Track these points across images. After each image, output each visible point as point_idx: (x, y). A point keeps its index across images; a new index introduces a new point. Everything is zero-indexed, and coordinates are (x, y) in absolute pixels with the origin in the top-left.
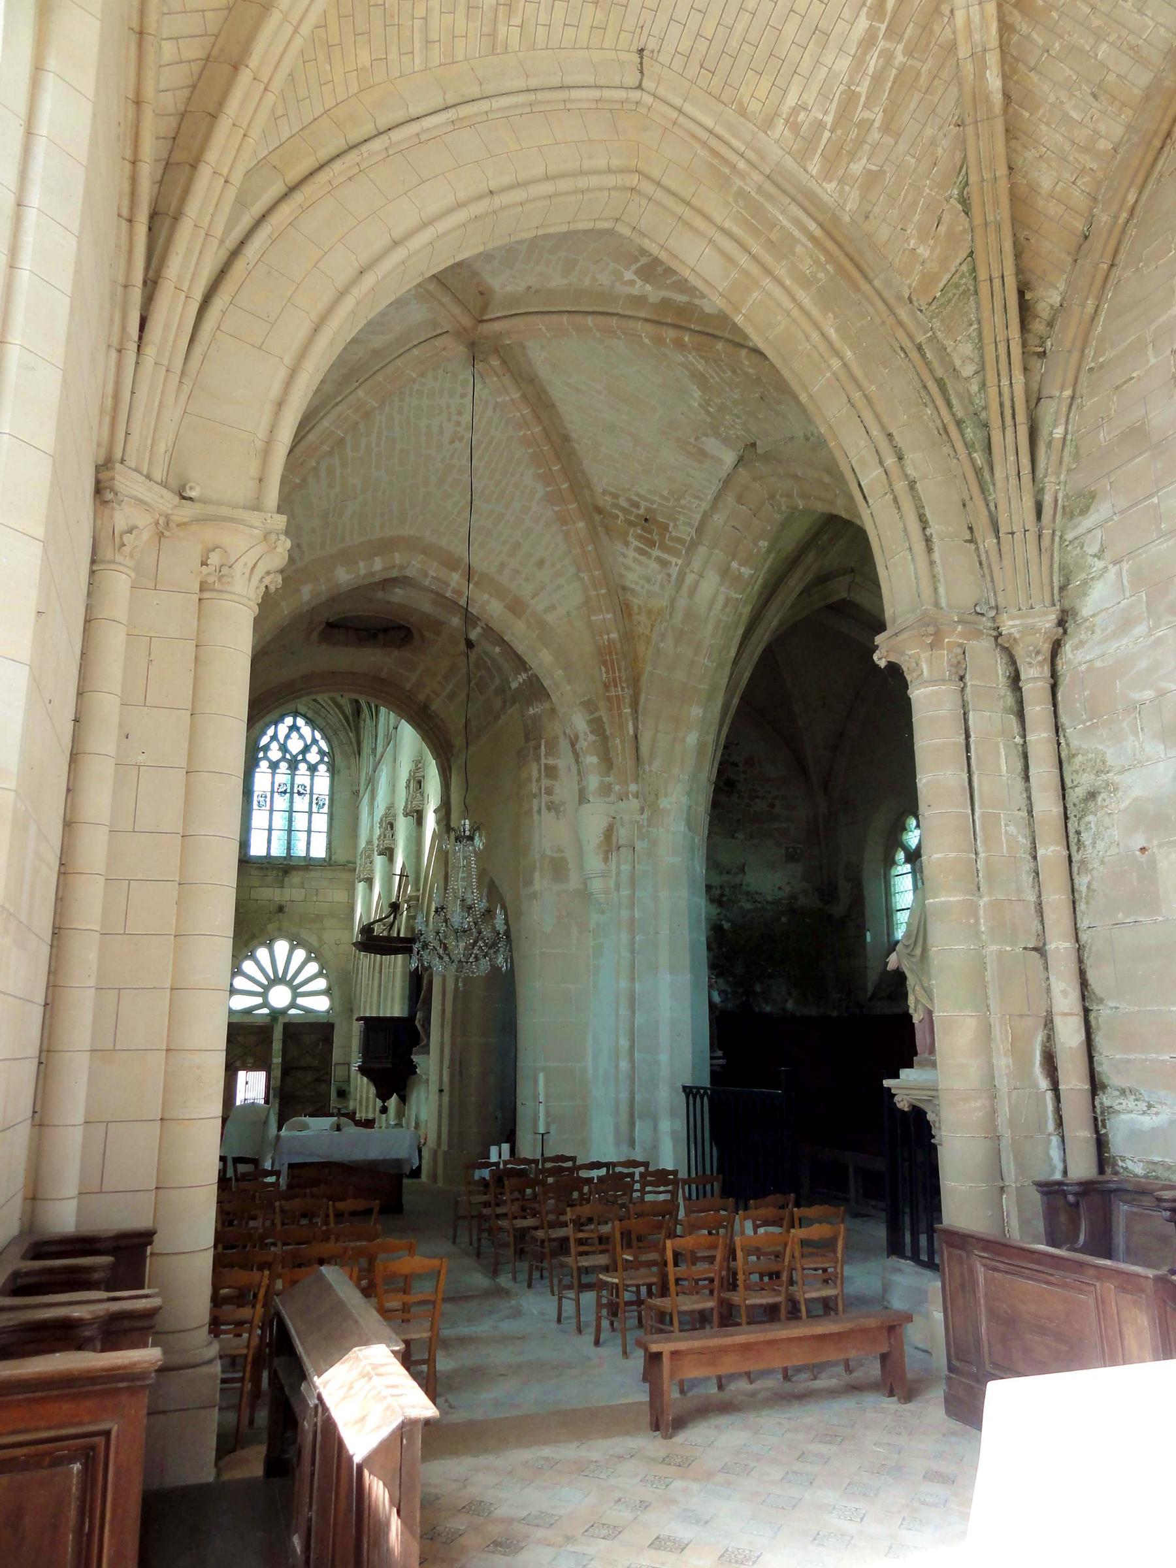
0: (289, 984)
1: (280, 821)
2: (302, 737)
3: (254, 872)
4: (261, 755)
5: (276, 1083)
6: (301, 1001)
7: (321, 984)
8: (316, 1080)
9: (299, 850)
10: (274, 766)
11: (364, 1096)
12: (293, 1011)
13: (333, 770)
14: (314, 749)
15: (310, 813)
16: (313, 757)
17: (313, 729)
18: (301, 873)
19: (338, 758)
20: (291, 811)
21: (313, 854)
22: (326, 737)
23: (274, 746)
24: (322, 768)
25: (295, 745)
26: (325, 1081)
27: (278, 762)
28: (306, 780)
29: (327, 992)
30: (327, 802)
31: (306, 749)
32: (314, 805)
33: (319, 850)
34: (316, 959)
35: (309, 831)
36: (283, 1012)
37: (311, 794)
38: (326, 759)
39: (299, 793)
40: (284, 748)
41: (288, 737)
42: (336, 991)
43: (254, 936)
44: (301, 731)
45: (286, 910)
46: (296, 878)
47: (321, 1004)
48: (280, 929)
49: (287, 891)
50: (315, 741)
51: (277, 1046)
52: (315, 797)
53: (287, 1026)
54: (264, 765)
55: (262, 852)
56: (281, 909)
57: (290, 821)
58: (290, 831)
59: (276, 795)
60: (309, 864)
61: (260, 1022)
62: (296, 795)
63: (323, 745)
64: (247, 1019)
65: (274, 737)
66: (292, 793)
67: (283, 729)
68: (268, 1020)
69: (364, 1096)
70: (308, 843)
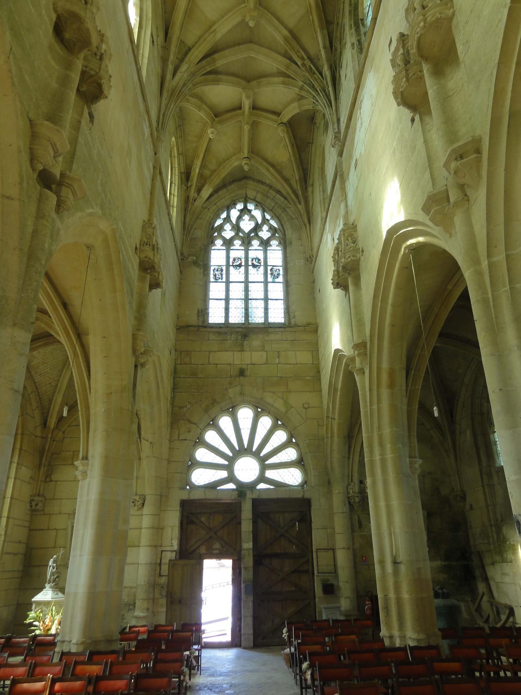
0: (256, 455)
1: (237, 291)
2: (252, 218)
3: (212, 337)
4: (216, 234)
5: (248, 575)
6: (270, 474)
7: (290, 454)
8: (294, 572)
9: (257, 317)
10: (228, 244)
11: (392, 595)
12: (262, 486)
13: (284, 244)
14: (265, 228)
15: (266, 283)
16: (265, 234)
17: (264, 211)
18: (260, 336)
19: (289, 233)
20: (247, 282)
21: (271, 320)
22: (275, 216)
23: (228, 227)
24: (274, 243)
25: (247, 225)
26: (307, 572)
27: (232, 239)
28: (260, 255)
29: (299, 463)
30: (281, 272)
31: (257, 228)
32: (269, 276)
33: (277, 315)
34: (284, 427)
35: (266, 299)
36: (252, 486)
37: (266, 265)
38: (277, 235)
39: (254, 266)
40: (237, 228)
41: (239, 218)
42: (309, 461)
43: (214, 402)
44: (253, 213)
45: (248, 373)
46: (255, 341)
47: (293, 477)
48: (242, 394)
49: (247, 354)
50: (265, 221)
51: (246, 527)
52: (269, 268)
53: (257, 503)
54: (219, 243)
55: (221, 320)
56: (242, 373)
57: (247, 290)
58: (247, 299)
59: (231, 268)
60: (267, 328)
61: (227, 499)
62: (250, 268)
63: (273, 223)
64: (211, 495)
65: (228, 219)
66: (247, 266)
67: (234, 214)
68: (235, 495)
69: (392, 595)
70: (266, 309)
